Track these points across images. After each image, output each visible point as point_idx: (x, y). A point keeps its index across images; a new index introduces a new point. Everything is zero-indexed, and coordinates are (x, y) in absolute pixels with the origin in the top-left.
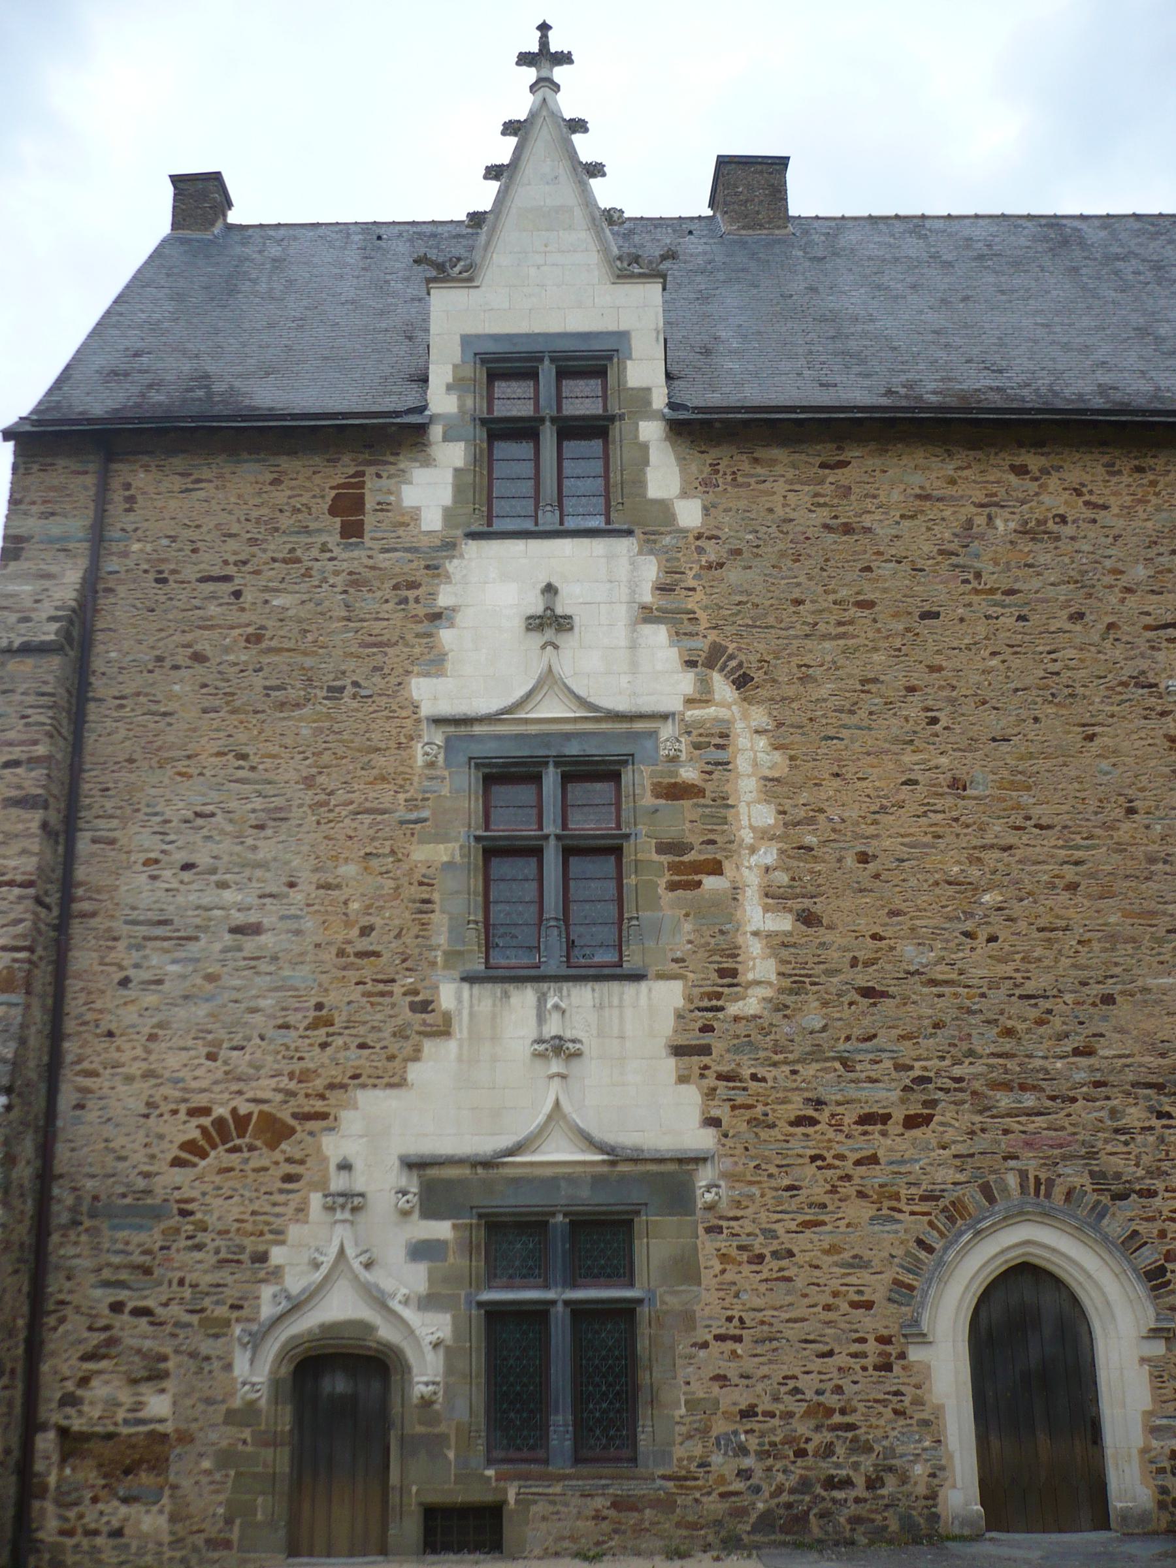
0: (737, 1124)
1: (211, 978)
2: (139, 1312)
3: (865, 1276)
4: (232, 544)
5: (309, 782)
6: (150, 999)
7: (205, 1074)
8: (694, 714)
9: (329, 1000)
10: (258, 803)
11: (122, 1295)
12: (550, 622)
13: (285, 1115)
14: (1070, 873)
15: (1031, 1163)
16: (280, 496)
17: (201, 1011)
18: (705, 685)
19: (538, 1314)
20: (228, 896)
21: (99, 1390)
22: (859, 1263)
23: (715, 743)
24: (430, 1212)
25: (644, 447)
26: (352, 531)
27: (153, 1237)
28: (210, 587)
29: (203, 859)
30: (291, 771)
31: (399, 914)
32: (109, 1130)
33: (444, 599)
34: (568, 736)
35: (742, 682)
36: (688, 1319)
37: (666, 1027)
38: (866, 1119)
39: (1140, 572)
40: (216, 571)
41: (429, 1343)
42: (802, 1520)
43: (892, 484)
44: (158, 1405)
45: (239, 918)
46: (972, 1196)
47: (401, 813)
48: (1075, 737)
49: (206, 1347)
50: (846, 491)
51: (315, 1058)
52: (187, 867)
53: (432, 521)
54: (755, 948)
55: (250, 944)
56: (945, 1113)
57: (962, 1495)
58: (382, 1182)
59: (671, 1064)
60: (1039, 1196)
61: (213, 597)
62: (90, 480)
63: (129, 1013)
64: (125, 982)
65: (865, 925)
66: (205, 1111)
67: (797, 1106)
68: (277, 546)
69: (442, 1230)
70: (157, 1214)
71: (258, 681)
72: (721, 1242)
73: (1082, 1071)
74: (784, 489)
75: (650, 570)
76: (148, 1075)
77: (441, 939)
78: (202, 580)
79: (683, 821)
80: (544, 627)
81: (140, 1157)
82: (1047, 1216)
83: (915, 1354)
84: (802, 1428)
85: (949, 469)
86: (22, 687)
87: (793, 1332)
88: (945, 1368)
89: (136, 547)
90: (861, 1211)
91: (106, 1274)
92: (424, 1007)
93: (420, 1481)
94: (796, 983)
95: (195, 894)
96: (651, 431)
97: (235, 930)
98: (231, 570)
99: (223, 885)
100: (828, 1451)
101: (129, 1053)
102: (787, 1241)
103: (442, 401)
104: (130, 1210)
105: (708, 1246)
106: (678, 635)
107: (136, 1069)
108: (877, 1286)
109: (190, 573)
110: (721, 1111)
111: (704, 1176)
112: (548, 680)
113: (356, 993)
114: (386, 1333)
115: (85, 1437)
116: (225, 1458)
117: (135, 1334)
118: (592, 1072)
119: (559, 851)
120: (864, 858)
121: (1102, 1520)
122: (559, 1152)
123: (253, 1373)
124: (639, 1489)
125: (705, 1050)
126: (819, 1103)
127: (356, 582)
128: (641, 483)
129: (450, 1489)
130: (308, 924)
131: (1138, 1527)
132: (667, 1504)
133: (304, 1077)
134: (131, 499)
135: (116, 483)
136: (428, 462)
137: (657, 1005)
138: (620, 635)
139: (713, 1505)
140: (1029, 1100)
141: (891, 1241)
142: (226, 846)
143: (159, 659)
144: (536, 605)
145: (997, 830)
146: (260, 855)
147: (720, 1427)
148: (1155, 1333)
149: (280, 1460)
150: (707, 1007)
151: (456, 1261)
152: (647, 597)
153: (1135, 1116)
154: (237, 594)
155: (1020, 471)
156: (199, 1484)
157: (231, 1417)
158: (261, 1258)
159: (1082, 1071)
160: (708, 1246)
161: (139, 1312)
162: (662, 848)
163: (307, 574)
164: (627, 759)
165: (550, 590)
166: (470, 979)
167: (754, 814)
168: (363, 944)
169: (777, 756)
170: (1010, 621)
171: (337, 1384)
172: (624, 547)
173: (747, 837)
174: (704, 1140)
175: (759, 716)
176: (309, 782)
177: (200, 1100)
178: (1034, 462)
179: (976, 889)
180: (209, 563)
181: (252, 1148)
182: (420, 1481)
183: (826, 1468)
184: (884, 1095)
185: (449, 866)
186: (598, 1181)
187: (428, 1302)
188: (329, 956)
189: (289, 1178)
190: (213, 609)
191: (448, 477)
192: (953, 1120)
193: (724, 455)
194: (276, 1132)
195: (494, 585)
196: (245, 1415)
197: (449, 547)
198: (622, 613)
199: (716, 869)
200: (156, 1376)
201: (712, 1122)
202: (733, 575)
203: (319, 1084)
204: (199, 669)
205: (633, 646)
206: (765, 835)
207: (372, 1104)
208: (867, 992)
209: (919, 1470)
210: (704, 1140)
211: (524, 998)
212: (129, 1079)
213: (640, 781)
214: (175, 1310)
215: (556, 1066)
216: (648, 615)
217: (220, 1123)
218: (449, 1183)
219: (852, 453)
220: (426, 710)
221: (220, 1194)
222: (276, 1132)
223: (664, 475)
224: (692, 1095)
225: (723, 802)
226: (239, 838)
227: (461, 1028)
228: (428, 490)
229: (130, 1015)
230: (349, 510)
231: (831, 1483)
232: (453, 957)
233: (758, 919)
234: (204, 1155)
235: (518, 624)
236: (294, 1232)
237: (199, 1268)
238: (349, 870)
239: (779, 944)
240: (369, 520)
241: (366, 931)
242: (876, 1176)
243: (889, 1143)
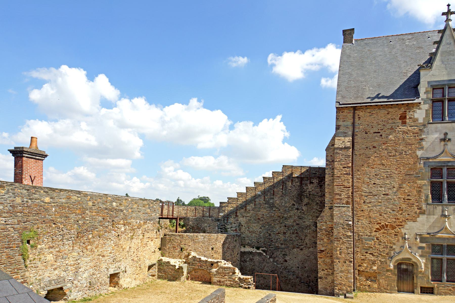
4: (380, 126)
26: (404, 123)
28: (376, 134)
40: (377, 131)
45: (384, 193)
51: (399, 216)
52: (374, 184)
55: (387, 197)
61: (376, 136)
66: (380, 224)
68: (389, 126)
89: (361, 127)
91: (365, 248)
98: (380, 131)
109: (372, 131)
134: (359, 118)
143: (367, 147)
154: (381, 135)
181: (389, 230)
190: (377, 138)
217: (383, 225)
234: (380, 230)
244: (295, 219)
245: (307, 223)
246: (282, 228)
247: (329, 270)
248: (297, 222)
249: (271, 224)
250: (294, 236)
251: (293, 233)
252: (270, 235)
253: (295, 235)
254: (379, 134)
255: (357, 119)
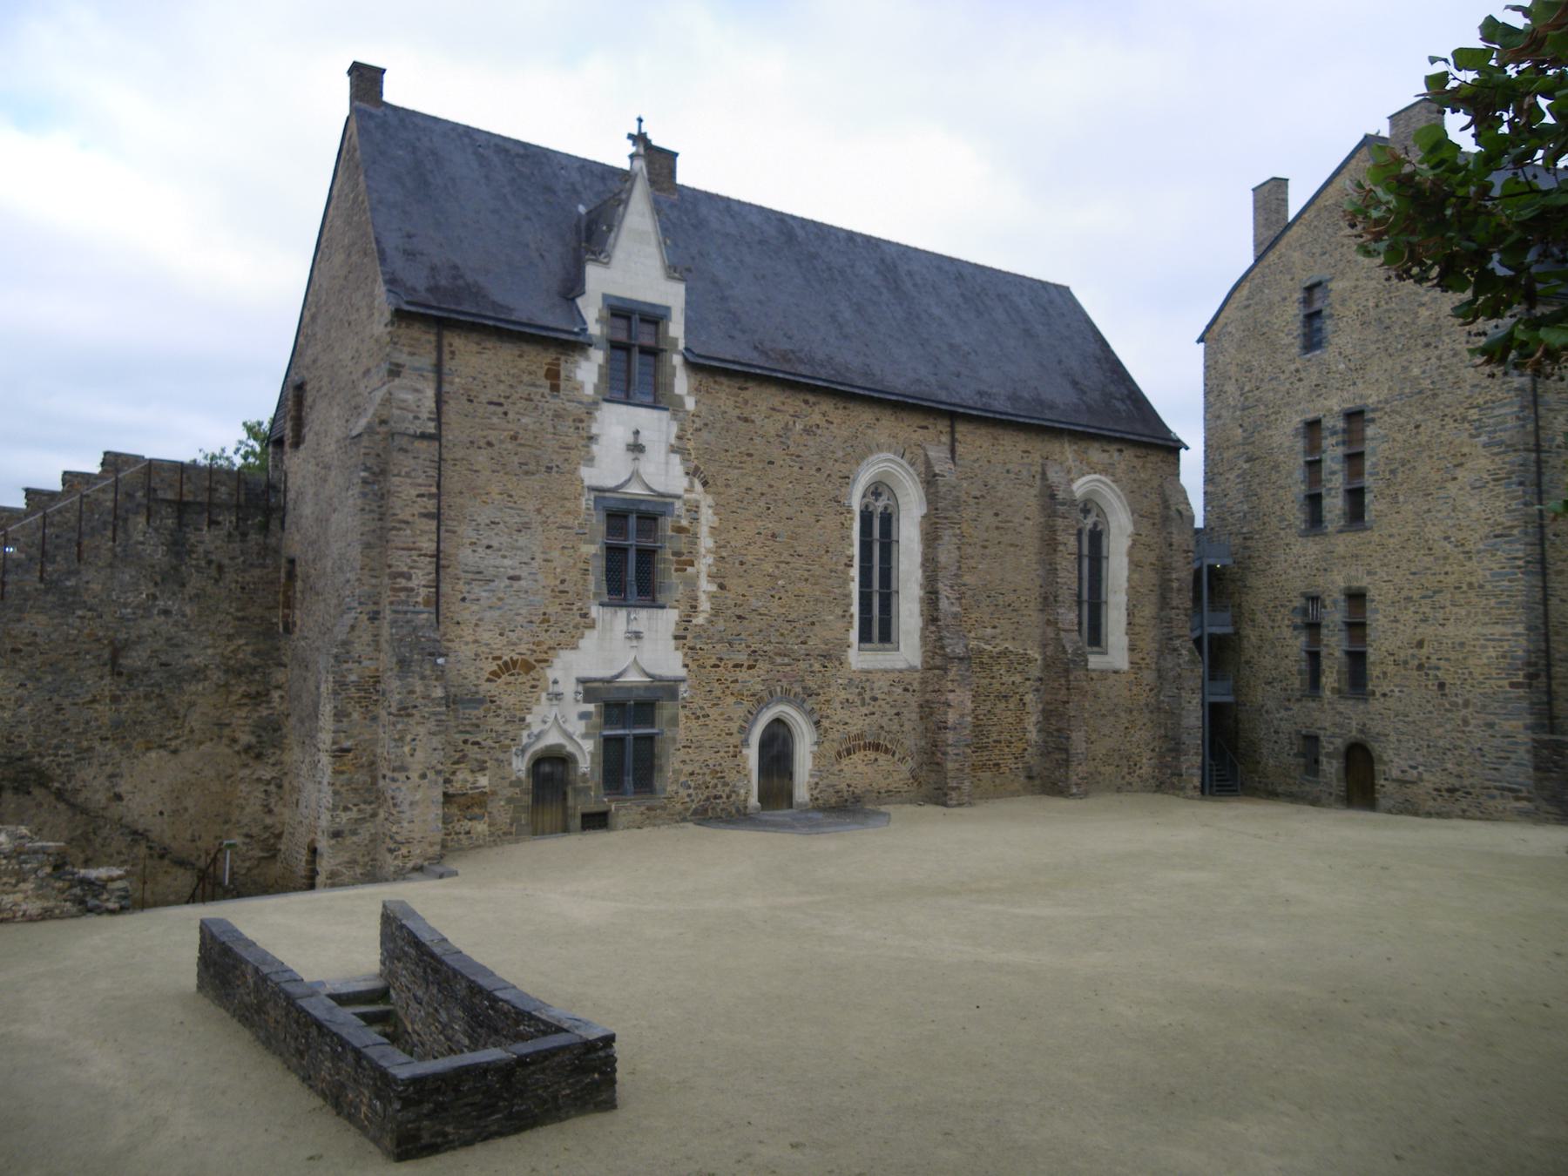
0: (693, 666)
1: (500, 599)
2: (475, 743)
3: (730, 724)
4: (502, 387)
5: (539, 511)
6: (475, 608)
7: (498, 643)
8: (686, 496)
9: (549, 610)
10: (517, 519)
11: (467, 736)
12: (636, 448)
13: (532, 660)
14: (806, 574)
15: (785, 684)
16: (523, 364)
17: (497, 613)
18: (692, 484)
19: (620, 740)
20: (507, 562)
21: (460, 776)
22: (730, 719)
23: (694, 509)
24: (587, 700)
25: (674, 368)
26: (555, 388)
27: (480, 712)
28: (493, 408)
29: (495, 544)
30: (531, 505)
31: (574, 575)
32: (459, 666)
33: (594, 430)
34: (642, 501)
35: (705, 484)
36: (674, 740)
37: (672, 628)
38: (736, 666)
39: (840, 454)
40: (495, 399)
41: (586, 754)
42: (706, 810)
43: (764, 400)
44: (483, 781)
45: (511, 573)
46: (765, 694)
47: (577, 529)
48: (812, 520)
49: (501, 756)
50: (746, 402)
51: (543, 636)
52: (489, 547)
53: (589, 389)
54: (703, 598)
55: (516, 584)
56: (760, 664)
57: (754, 801)
58: (569, 688)
59: (673, 643)
60: (787, 697)
61: (494, 413)
62: (432, 338)
63: (466, 613)
64: (464, 599)
65: (740, 591)
66: (499, 658)
67: (713, 661)
68: (523, 390)
69: (591, 707)
70: (481, 701)
71: (516, 459)
72: (687, 712)
73: (802, 649)
74: (725, 397)
75: (674, 429)
76: (476, 641)
77: (592, 587)
78: (490, 403)
79: (682, 543)
80: (633, 448)
81: (473, 677)
82: (789, 702)
83: (745, 751)
84: (708, 778)
85: (782, 398)
86: (423, 456)
87: (707, 744)
88: (752, 755)
90: (731, 700)
92: (585, 616)
93: (580, 805)
94: (716, 612)
95: (492, 560)
96: (677, 360)
97: (511, 578)
98: (502, 400)
99: (504, 557)
100: (715, 786)
101: (467, 632)
102: (707, 711)
103: (594, 329)
104: (470, 701)
105: (682, 713)
106: (685, 460)
107: (470, 639)
108: (734, 727)
109: (483, 398)
110: (689, 662)
111: (682, 687)
112: (635, 475)
113: (558, 609)
114: (570, 748)
115: (454, 796)
116: (510, 800)
117: (473, 752)
118: (646, 644)
119: (633, 551)
120: (742, 563)
121: (790, 806)
122: (634, 677)
123: (520, 766)
124: (656, 803)
125: (684, 638)
126: (721, 659)
127: (557, 415)
128: (672, 385)
129: (593, 807)
130: (539, 577)
131: (804, 809)
132: (664, 808)
133: (539, 644)
134: (453, 353)
135: (445, 342)
136: (588, 359)
137: (668, 618)
138: (662, 457)
139: (679, 807)
140: (786, 660)
141: (740, 712)
142: (505, 539)
144: (631, 440)
145: (785, 556)
146: (520, 544)
147: (683, 779)
148: (817, 743)
149: (528, 799)
150: (686, 620)
151: (596, 720)
152: (673, 441)
153: (817, 667)
154: (506, 414)
155: (806, 402)
156: (500, 810)
157: (512, 784)
158: (523, 720)
159: (802, 649)
160: (682, 713)
161: (475, 743)
162: (675, 554)
163: (536, 408)
164: (663, 514)
165: (637, 433)
166: (602, 605)
167: (706, 542)
168: (562, 587)
169: (716, 518)
170: (796, 469)
171: (546, 768)
172: (665, 415)
173: (703, 551)
174: (682, 672)
175: (709, 500)
176: (539, 511)
177: (497, 653)
178: (812, 399)
179: (777, 579)
180: (491, 394)
182: (580, 805)
183: (715, 792)
184: (742, 658)
185: (595, 555)
186: (647, 688)
187: (585, 736)
188: (548, 592)
189: (533, 687)
190: (495, 420)
191: (596, 369)
192: (763, 666)
193: (708, 381)
194: (528, 667)
195: (616, 424)
196: (517, 783)
197: (596, 403)
198: (663, 448)
199: (692, 564)
200: (481, 768)
201: (686, 666)
202: (705, 434)
203: (545, 647)
204: (490, 450)
205: (667, 463)
206: (709, 551)
207: (565, 656)
208: (739, 617)
209: (742, 792)
210: (682, 672)
211: (622, 614)
212: (467, 643)
213: (667, 524)
214: (490, 742)
215: (635, 643)
216: (673, 450)
217: (506, 663)
218: (595, 689)
219: (749, 384)
220: (587, 483)
221: (506, 693)
222: (528, 667)
223: (682, 383)
224: (679, 655)
225: (696, 536)
226: (510, 535)
227: (599, 625)
228: (587, 372)
229: (466, 615)
230: (553, 375)
231: (716, 797)
232: (596, 595)
233: (706, 586)
235: (623, 447)
236: (535, 709)
237: (498, 724)
238: (555, 554)
239: (712, 596)
240: (562, 384)
241: (563, 582)
242: (738, 686)
243: (742, 675)
244: (156, 646)
245: (198, 660)
246: (108, 680)
247: (362, 806)
248: (163, 658)
249: (64, 670)
250: (148, 706)
251: (147, 697)
252: (59, 709)
253: (154, 703)
254: (500, 410)
255: (446, 356)
